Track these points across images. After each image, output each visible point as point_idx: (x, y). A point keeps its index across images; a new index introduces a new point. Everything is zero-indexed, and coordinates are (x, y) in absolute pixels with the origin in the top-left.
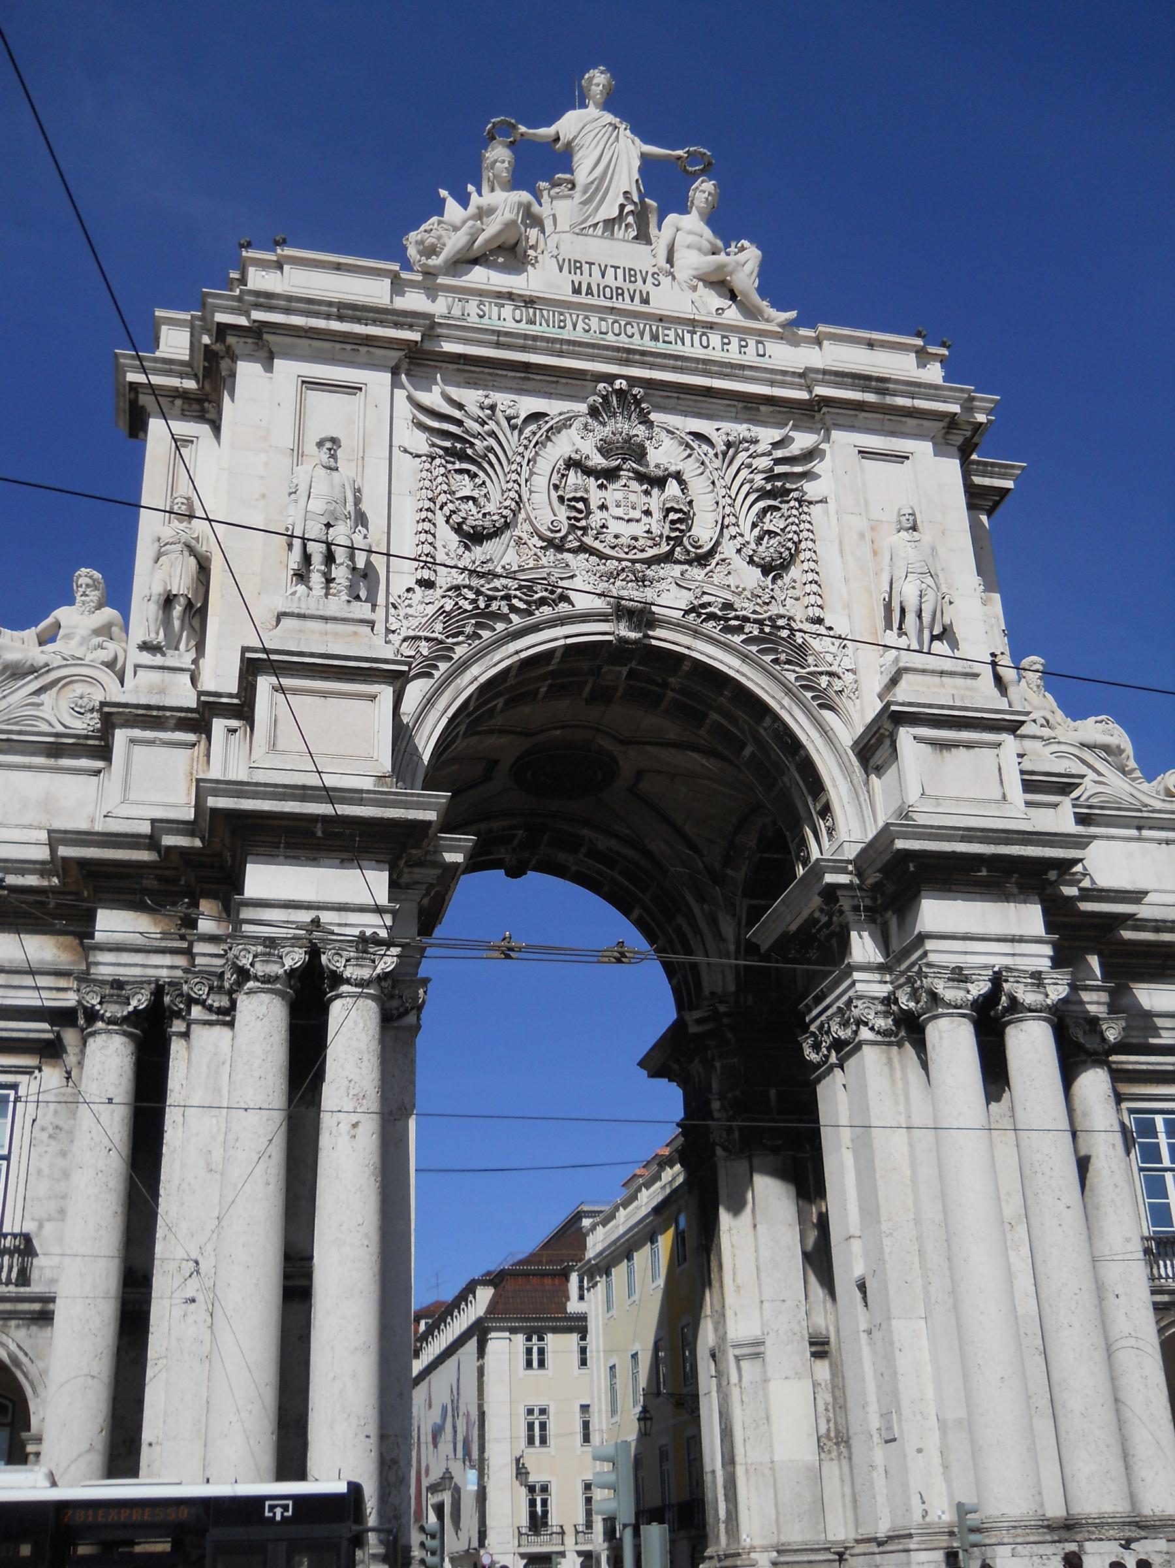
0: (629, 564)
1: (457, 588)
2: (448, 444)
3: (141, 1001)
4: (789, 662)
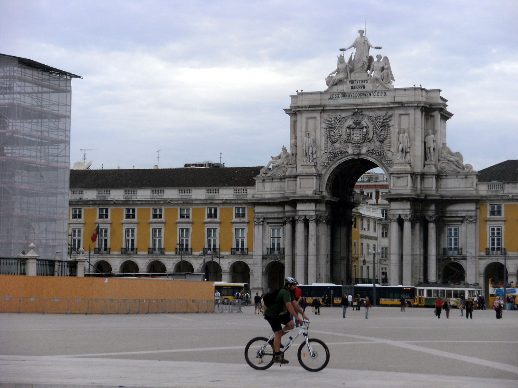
0: (357, 144)
1: (330, 153)
3: (291, 219)
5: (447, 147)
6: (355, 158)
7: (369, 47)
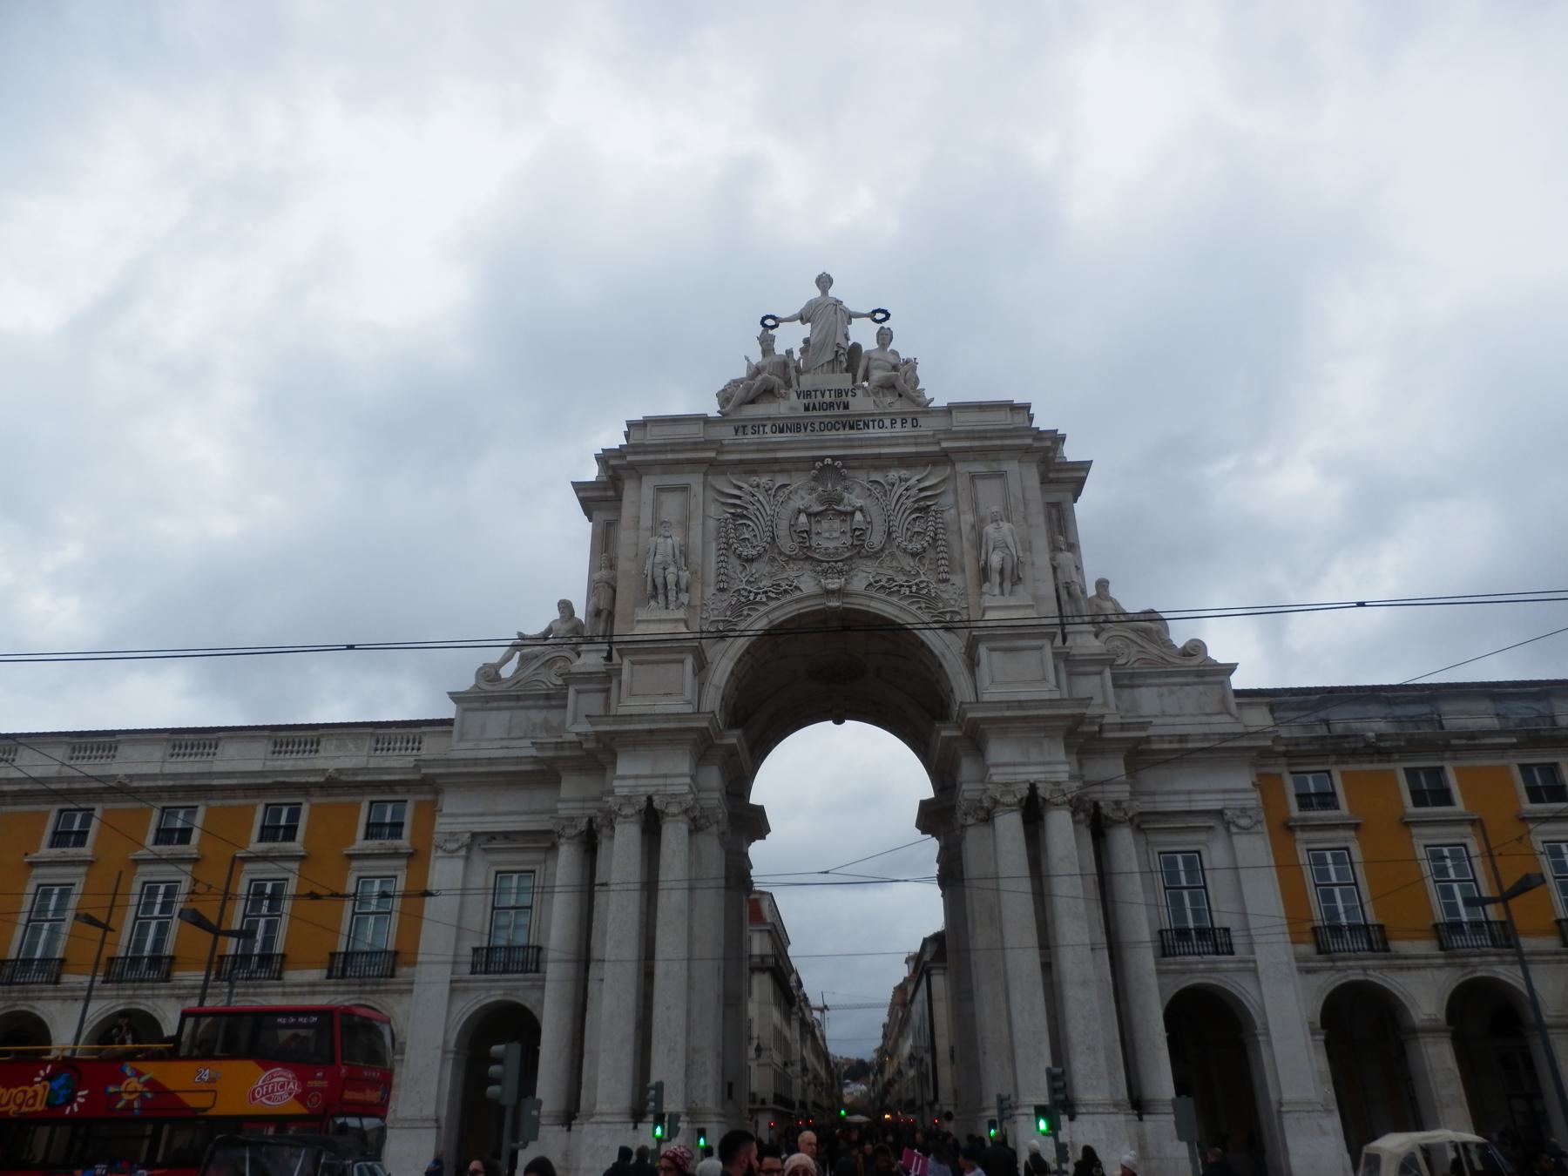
1: (739, 590)
2: (733, 511)
4: (927, 608)
5: (1112, 600)
6: (830, 604)
7: (850, 318)
